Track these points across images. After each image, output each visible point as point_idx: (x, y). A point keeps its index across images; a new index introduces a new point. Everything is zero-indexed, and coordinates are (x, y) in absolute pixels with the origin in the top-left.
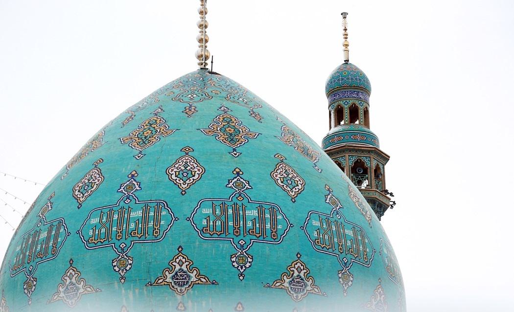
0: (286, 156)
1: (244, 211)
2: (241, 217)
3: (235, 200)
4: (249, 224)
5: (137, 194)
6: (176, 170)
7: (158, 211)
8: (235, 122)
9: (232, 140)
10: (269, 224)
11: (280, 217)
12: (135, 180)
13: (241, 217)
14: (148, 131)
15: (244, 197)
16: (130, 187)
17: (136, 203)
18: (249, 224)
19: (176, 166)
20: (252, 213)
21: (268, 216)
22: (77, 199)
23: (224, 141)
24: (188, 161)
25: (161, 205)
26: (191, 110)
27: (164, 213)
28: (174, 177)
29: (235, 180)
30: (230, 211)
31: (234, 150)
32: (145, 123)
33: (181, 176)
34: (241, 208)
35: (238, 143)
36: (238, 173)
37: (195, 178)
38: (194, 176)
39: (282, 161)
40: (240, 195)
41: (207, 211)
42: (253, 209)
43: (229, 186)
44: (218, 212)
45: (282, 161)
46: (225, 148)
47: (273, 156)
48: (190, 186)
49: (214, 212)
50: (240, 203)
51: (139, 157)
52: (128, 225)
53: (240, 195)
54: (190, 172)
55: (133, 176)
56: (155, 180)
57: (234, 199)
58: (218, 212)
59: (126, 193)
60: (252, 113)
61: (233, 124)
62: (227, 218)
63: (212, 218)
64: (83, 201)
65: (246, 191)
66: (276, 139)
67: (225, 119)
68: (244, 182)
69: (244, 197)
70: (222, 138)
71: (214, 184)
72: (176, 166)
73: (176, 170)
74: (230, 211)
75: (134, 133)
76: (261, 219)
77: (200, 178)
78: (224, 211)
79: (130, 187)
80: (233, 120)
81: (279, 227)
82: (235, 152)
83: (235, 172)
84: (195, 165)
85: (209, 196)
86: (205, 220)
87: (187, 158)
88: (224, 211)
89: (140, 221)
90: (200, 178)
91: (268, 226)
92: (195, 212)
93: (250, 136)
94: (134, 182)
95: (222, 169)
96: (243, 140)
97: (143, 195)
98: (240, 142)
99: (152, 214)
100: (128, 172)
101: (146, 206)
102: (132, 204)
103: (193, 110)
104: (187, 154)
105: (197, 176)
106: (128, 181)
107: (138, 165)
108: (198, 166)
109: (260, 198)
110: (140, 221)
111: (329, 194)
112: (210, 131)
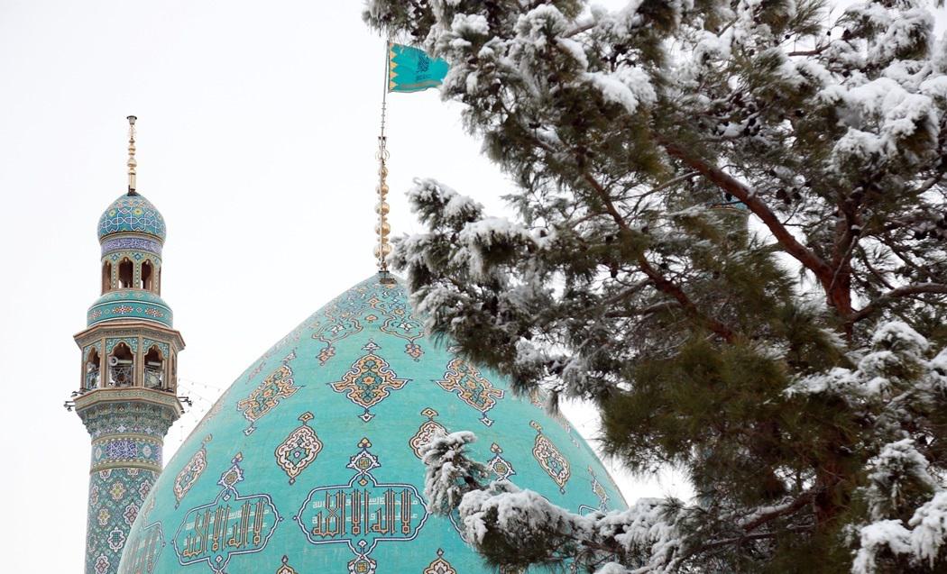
0: (439, 410)
1: (367, 499)
2: (363, 508)
3: (356, 484)
4: (373, 517)
5: (238, 486)
6: (287, 449)
7: (260, 510)
8: (379, 366)
9: (368, 395)
10: (399, 514)
11: (415, 502)
12: (238, 467)
13: (363, 508)
14: (369, 378)
15: (368, 480)
16: (231, 478)
17: (374, 486)
18: (373, 517)
19: (289, 443)
20: (378, 501)
21: (398, 503)
22: (176, 494)
23: (357, 398)
24: (304, 434)
25: (265, 500)
26: (326, 354)
27: (267, 512)
28: (283, 460)
29: (360, 456)
30: (349, 502)
31: (367, 411)
32: (359, 364)
33: (291, 458)
34: (363, 496)
35: (374, 399)
36: (365, 446)
37: (283, 458)
38: (307, 456)
39: (431, 419)
40: (363, 478)
41: (318, 504)
42: (379, 495)
43: (351, 466)
44: (333, 505)
45: (431, 419)
46: (355, 409)
47: (419, 413)
48: (301, 470)
49: (328, 505)
50: (362, 490)
51: (366, 418)
52: (367, 518)
53: (363, 478)
54: (303, 451)
55: (365, 446)
56: (261, 465)
57: (356, 484)
58: (333, 505)
59: (226, 485)
60: (409, 346)
61: (376, 370)
62: (343, 511)
63: (325, 513)
64: (182, 498)
65: (373, 472)
66: (433, 386)
67: (367, 364)
68: (371, 458)
69: (368, 480)
70: (354, 395)
71: (332, 469)
72: (289, 443)
73: (287, 449)
74: (349, 502)
75: (350, 378)
76: (389, 508)
77: (314, 459)
78: (341, 502)
79: (231, 478)
80: (378, 362)
81: (414, 516)
82: (367, 415)
83: (361, 445)
84: (312, 440)
85: (323, 484)
86: (316, 518)
87: (303, 430)
88: (341, 502)
89: (383, 511)
90: (314, 459)
91: (398, 517)
92: (303, 506)
93: (396, 384)
94: (237, 470)
95: (344, 443)
96: (382, 394)
97: (244, 488)
98: (378, 397)
99: (253, 514)
100: (233, 455)
101: (247, 503)
102: (231, 503)
103: (330, 354)
104: (305, 423)
105: (311, 455)
106: (360, 453)
107: (245, 445)
108: (314, 441)
109: (389, 479)
110: (383, 511)
111: (495, 458)
112: (343, 386)
